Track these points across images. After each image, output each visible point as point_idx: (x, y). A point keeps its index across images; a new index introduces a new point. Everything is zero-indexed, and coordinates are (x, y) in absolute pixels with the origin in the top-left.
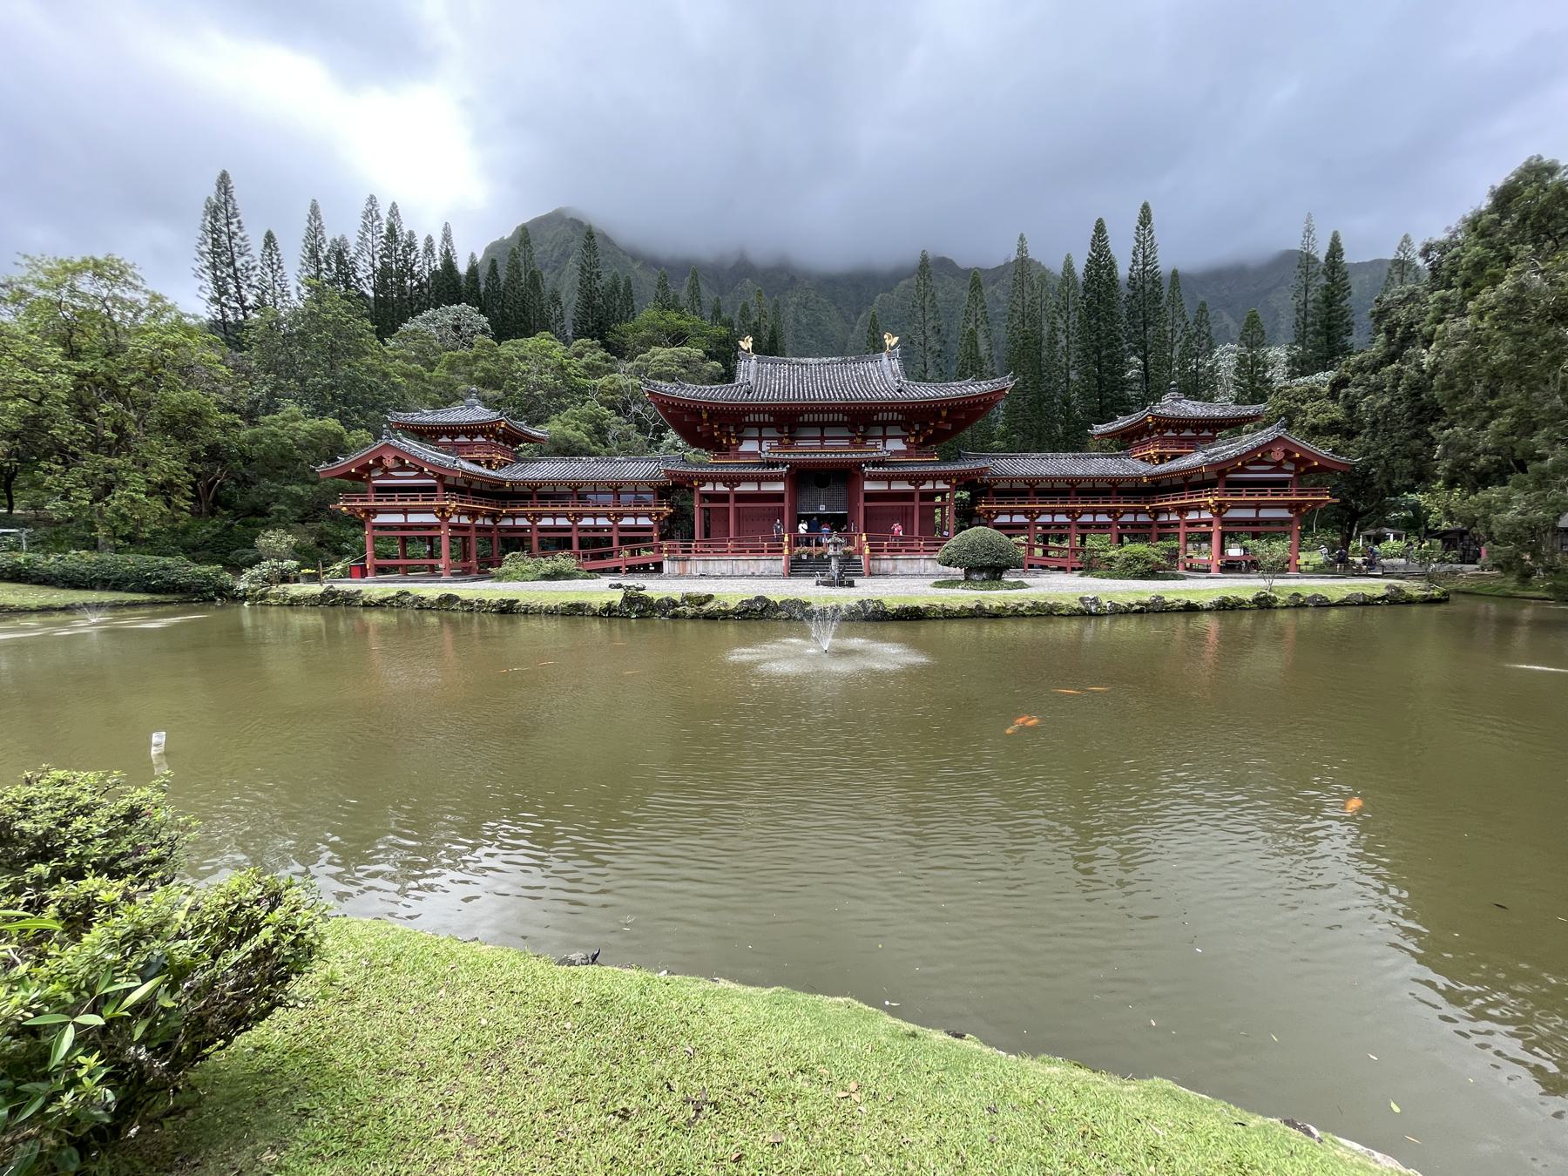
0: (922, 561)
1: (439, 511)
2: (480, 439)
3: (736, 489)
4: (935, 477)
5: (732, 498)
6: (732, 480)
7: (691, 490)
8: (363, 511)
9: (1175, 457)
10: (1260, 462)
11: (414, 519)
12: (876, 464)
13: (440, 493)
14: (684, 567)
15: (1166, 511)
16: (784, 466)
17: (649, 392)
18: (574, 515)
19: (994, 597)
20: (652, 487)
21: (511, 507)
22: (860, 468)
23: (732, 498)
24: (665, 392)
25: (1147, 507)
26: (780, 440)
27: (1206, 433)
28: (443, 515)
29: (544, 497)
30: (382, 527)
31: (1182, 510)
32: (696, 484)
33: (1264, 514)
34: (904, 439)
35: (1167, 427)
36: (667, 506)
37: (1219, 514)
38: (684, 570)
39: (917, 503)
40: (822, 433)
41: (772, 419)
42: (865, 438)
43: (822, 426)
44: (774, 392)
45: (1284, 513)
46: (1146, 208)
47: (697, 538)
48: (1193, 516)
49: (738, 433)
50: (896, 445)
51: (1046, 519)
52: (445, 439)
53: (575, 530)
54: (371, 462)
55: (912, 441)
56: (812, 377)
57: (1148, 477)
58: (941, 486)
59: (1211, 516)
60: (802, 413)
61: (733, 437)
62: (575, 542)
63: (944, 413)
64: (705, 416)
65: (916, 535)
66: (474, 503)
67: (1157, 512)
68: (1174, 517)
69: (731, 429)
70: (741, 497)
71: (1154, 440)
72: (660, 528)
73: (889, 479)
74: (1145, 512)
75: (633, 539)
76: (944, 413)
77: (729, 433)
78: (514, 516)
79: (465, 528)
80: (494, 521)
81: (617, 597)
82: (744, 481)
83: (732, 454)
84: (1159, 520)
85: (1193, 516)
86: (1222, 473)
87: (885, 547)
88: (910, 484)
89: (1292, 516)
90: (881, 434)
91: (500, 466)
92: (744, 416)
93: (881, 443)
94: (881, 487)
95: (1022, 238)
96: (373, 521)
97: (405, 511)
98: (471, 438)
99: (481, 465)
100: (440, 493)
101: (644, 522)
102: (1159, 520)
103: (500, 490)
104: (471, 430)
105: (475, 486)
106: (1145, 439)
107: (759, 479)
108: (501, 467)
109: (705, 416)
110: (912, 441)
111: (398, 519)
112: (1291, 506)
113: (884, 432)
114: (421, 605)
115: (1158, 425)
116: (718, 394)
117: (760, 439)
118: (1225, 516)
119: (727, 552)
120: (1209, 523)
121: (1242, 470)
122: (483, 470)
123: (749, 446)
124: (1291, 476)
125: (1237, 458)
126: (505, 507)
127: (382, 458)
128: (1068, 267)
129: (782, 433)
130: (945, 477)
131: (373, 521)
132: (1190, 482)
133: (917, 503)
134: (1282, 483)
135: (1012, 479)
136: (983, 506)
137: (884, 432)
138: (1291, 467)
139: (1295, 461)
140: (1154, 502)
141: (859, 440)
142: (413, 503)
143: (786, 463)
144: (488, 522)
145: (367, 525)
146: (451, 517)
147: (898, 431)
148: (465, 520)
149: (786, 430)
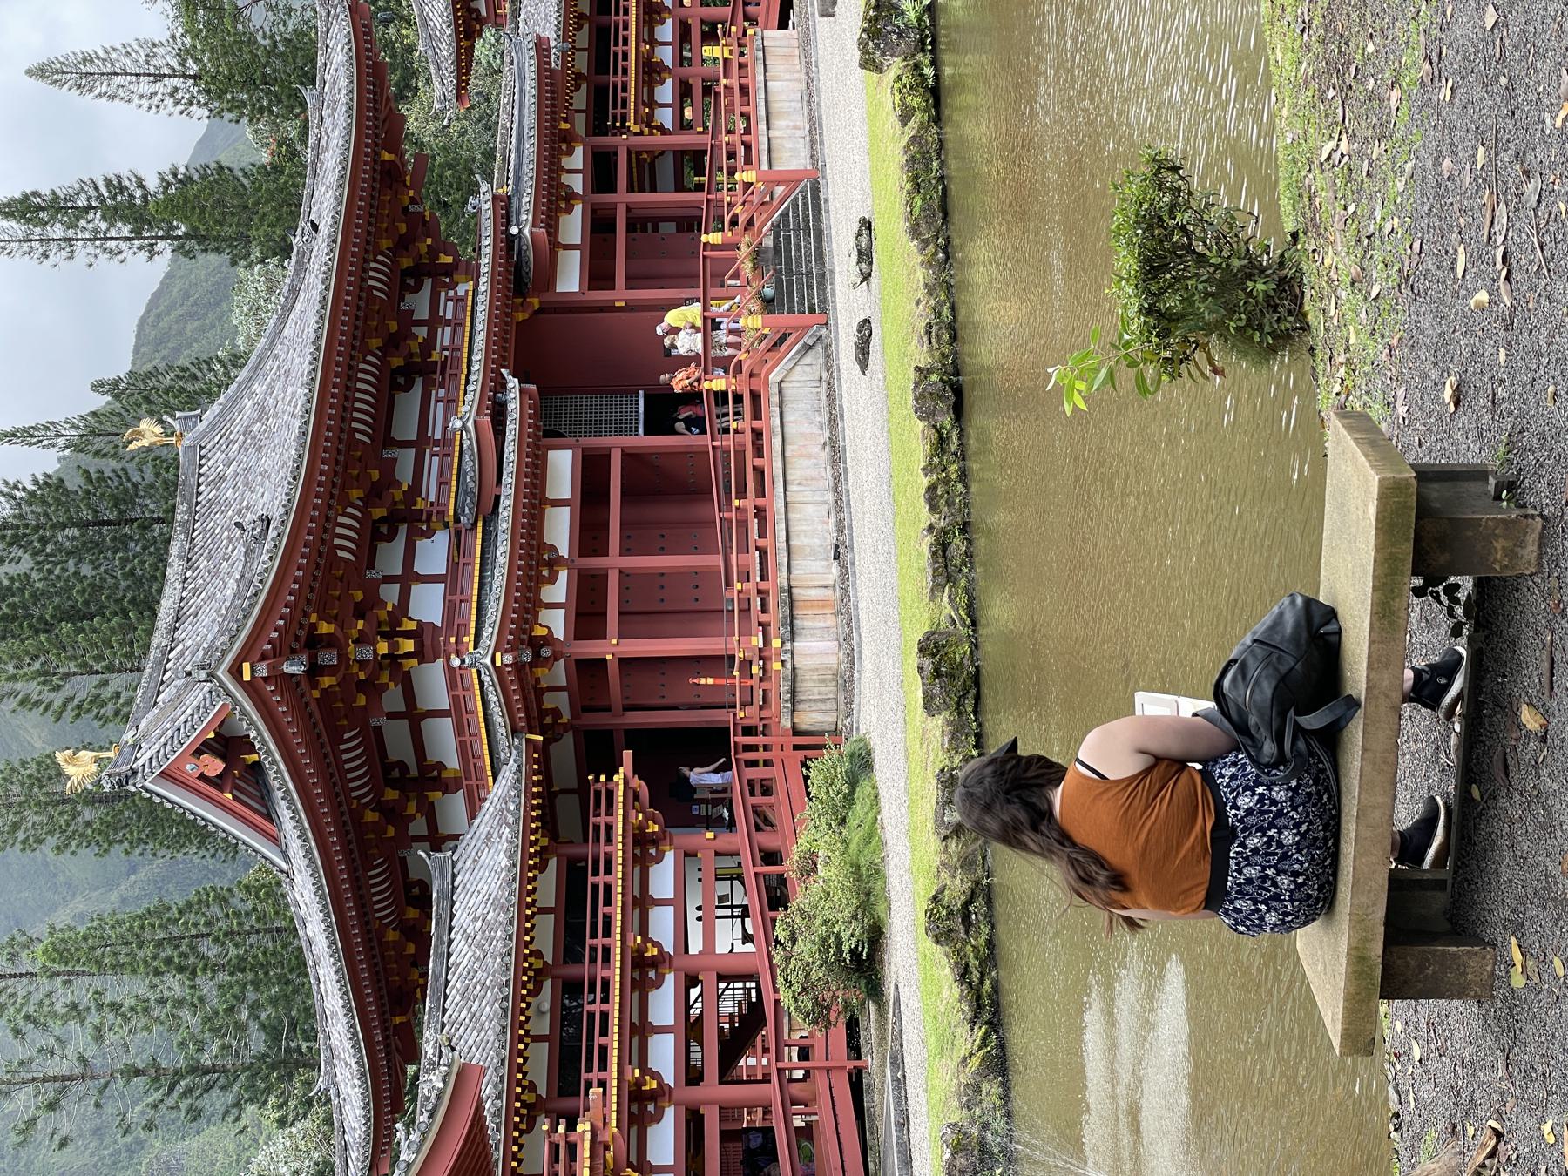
3: (564, 551)
4: (550, 168)
14: (812, 603)
16: (502, 385)
32: (544, 632)
36: (609, 779)
38: (824, 603)
58: (577, 159)
63: (386, 156)
64: (325, 628)
65: (703, 196)
70: (590, 535)
73: (555, 245)
76: (386, 156)
87: (736, 139)
88: (569, 210)
92: (333, 561)
107: (535, 501)
117: (409, 577)
119: (760, 513)
123: (428, 605)
130: (554, 143)
133: (622, 198)
137: (420, 323)
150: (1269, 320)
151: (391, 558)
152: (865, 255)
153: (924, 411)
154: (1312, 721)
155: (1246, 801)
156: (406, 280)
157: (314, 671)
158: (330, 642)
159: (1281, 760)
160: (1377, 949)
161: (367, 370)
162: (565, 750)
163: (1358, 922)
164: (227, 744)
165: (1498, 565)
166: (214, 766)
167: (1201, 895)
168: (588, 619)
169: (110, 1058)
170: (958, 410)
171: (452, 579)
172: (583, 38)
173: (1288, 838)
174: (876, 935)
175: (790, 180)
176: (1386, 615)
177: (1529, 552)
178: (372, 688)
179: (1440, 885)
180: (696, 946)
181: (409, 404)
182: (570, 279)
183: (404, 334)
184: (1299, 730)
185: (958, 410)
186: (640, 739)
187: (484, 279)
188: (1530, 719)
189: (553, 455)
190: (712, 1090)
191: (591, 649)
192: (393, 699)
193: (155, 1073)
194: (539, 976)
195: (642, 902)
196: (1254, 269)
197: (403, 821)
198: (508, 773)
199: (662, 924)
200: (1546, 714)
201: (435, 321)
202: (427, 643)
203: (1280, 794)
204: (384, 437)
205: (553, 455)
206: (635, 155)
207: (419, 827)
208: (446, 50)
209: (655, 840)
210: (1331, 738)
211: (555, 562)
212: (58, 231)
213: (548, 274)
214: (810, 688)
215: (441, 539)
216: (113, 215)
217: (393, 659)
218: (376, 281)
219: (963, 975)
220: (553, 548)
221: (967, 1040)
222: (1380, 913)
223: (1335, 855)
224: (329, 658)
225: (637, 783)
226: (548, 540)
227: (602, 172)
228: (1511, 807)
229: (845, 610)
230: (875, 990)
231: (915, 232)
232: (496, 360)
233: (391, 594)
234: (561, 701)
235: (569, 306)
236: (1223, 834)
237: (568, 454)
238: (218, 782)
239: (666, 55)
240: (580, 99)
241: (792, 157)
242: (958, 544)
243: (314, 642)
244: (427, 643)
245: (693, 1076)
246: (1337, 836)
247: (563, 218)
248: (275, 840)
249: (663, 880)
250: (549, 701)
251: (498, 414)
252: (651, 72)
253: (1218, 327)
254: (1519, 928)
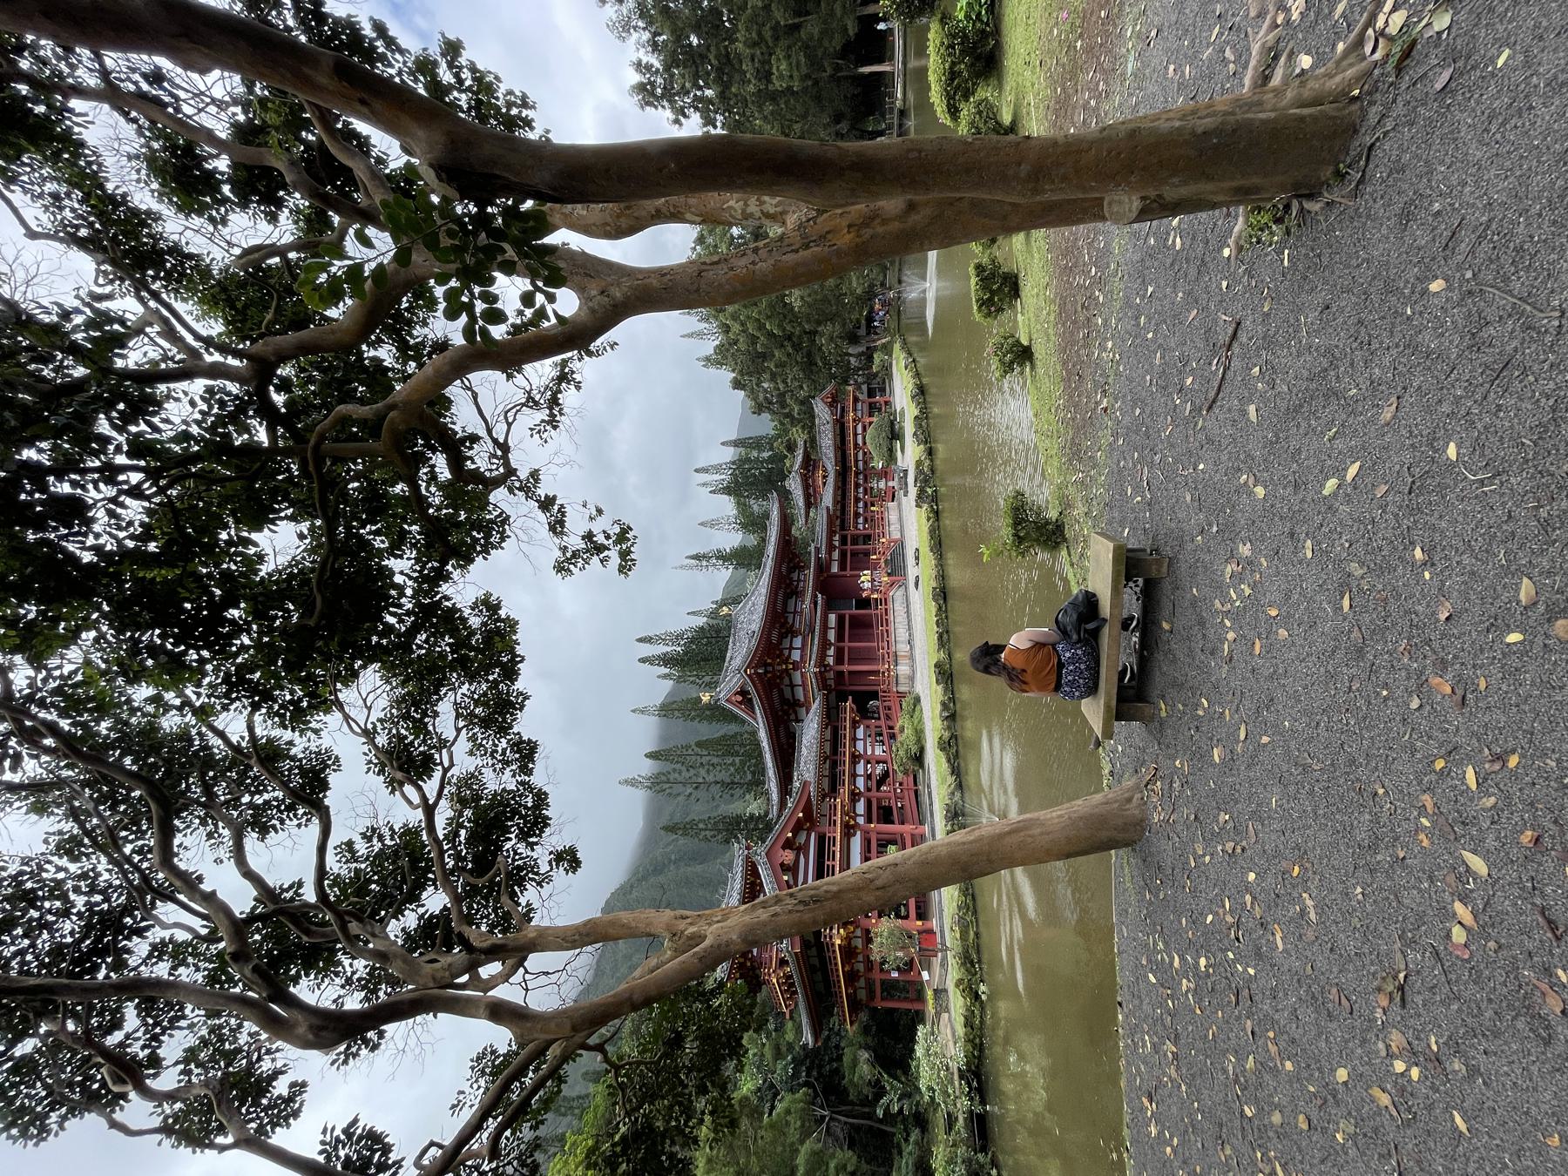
6: (825, 645)
15: (856, 461)
19: (909, 428)
31: (856, 444)
46: (640, 640)
51: (860, 782)
53: (869, 794)
58: (837, 537)
70: (840, 637)
71: (814, 481)
73: (831, 560)
95: (633, 711)
117: (791, 648)
123: (796, 655)
127: (782, 865)
128: (665, 676)
130: (831, 533)
133: (849, 547)
134: (843, 409)
150: (1054, 538)
151: (786, 643)
152: (917, 558)
153: (934, 599)
154: (1091, 626)
155: (1068, 655)
156: (791, 570)
157: (766, 672)
158: (770, 665)
159: (1079, 641)
160: (1114, 703)
161: (781, 593)
162: (833, 696)
163: (1108, 694)
164: (743, 692)
165: (1154, 574)
166: (740, 698)
167: (1053, 686)
168: (839, 659)
169: (710, 778)
170: (945, 599)
171: (803, 649)
172: (839, 507)
173: (1083, 667)
174: (922, 750)
175: (895, 541)
176: (1116, 591)
177: (1164, 569)
178: (781, 678)
179: (1132, 687)
180: (869, 752)
181: (792, 602)
182: (835, 569)
183: (791, 584)
184: (1086, 630)
185: (945, 599)
186: (853, 693)
188: (1166, 626)
190: (874, 793)
191: (840, 668)
192: (786, 681)
193: (723, 783)
194: (825, 760)
195: (854, 739)
196: (1048, 523)
197: (789, 715)
198: (817, 701)
199: (860, 746)
200: (1172, 623)
201: (799, 580)
202: (796, 666)
203: (1079, 652)
206: (852, 536)
207: (793, 717)
208: (803, 512)
209: (858, 722)
210: (1095, 634)
211: (831, 644)
212: (704, 563)
213: (829, 567)
214: (901, 680)
215: (800, 638)
216: (717, 558)
217: (787, 670)
218: (784, 569)
219: (949, 761)
221: (951, 779)
222: (1115, 691)
223: (1098, 672)
224: (770, 669)
227: (843, 540)
228: (1160, 656)
229: (912, 658)
230: (922, 765)
231: (931, 550)
232: (815, 589)
233: (786, 652)
234: (831, 683)
235: (835, 576)
236: (1061, 665)
238: (740, 703)
239: (861, 511)
240: (838, 522)
241: (896, 535)
242: (945, 636)
244: (796, 666)
245: (869, 790)
246: (1099, 666)
248: (755, 719)
249: (860, 733)
250: (829, 682)
251: (816, 604)
252: (857, 515)
253: (1037, 540)
254: (1163, 697)
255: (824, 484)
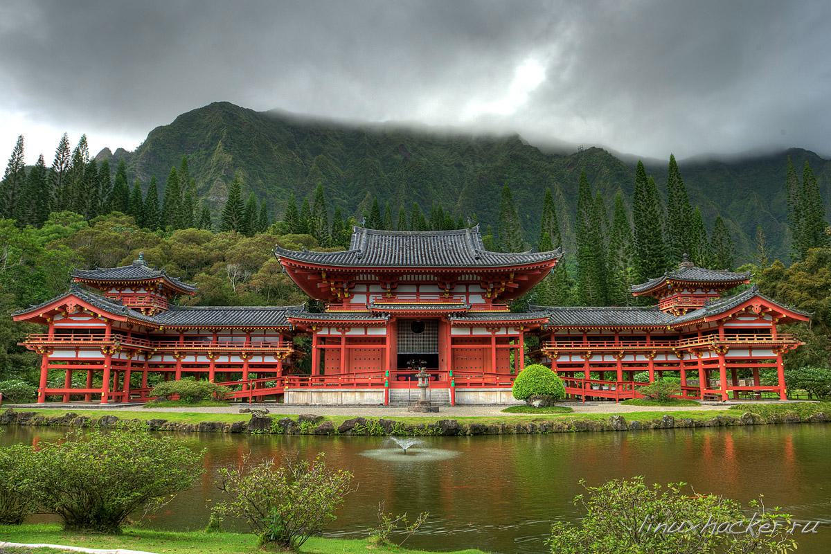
0: (499, 393)
1: (105, 349)
2: (142, 291)
3: (347, 334)
5: (343, 342)
7: (310, 334)
8: (43, 348)
9: (691, 310)
10: (748, 313)
11: (83, 355)
12: (458, 315)
13: (107, 334)
16: (386, 315)
17: (281, 258)
18: (213, 353)
20: (278, 331)
21: (162, 346)
22: (447, 318)
23: (343, 342)
24: (294, 258)
25: (674, 349)
26: (384, 294)
27: (712, 292)
28: (108, 352)
29: (189, 338)
30: (55, 361)
31: (698, 351)
33: (756, 354)
34: (483, 294)
35: (683, 287)
37: (722, 354)
39: (493, 345)
40: (418, 289)
41: (377, 278)
42: (451, 294)
43: (418, 284)
44: (380, 257)
45: (770, 354)
47: (313, 373)
48: (706, 356)
49: (350, 289)
50: (476, 300)
52: (114, 291)
54: (56, 309)
55: (489, 296)
56: (410, 246)
57: (671, 326)
58: (512, 332)
59: (717, 356)
60: (401, 274)
61: (346, 293)
62: (212, 375)
63: (512, 276)
64: (324, 276)
66: (133, 343)
67: (682, 352)
68: (694, 358)
69: (345, 286)
70: (351, 340)
72: (283, 367)
74: (673, 353)
75: (264, 372)
77: (343, 289)
78: (162, 354)
79: (123, 363)
80: (146, 358)
81: (247, 418)
82: (354, 327)
83: (344, 305)
84: (684, 359)
85: (706, 356)
86: (720, 322)
88: (488, 330)
89: (776, 355)
90: (465, 291)
91: (156, 313)
93: (465, 299)
94: (465, 333)
96: (50, 356)
97: (77, 349)
98: (135, 291)
99: (141, 312)
100: (107, 334)
101: (270, 360)
102: (684, 359)
103: (151, 333)
104: (135, 285)
105: (135, 329)
106: (669, 296)
107: (366, 326)
108: (156, 314)
109: (324, 276)
110: (489, 296)
111: (71, 355)
112: (776, 348)
113: (467, 289)
114: (86, 425)
115: (675, 286)
116: (334, 257)
117: (368, 294)
118: (726, 356)
120: (716, 362)
121: (734, 319)
122: (143, 316)
123: (358, 299)
124: (771, 325)
125: (728, 311)
126: (157, 346)
127: (66, 306)
129: (386, 289)
130: (516, 326)
131: (50, 356)
132: (698, 330)
135: (568, 327)
136: (547, 348)
138: (770, 319)
139: (769, 313)
140: (678, 345)
141: (447, 295)
142: (86, 342)
143: (388, 313)
144: (142, 359)
145: (44, 360)
146: (114, 354)
147: (477, 289)
148: (124, 357)
149: (388, 286)
181: (436, 289)
187: (425, 308)
189: (385, 329)
204: (467, 284)
205: (385, 330)
220: (349, 331)
225: (288, 354)
226: (351, 329)
237: (385, 333)
243: (320, 273)
247: (485, 329)
251: (378, 314)
255: (668, 312)
